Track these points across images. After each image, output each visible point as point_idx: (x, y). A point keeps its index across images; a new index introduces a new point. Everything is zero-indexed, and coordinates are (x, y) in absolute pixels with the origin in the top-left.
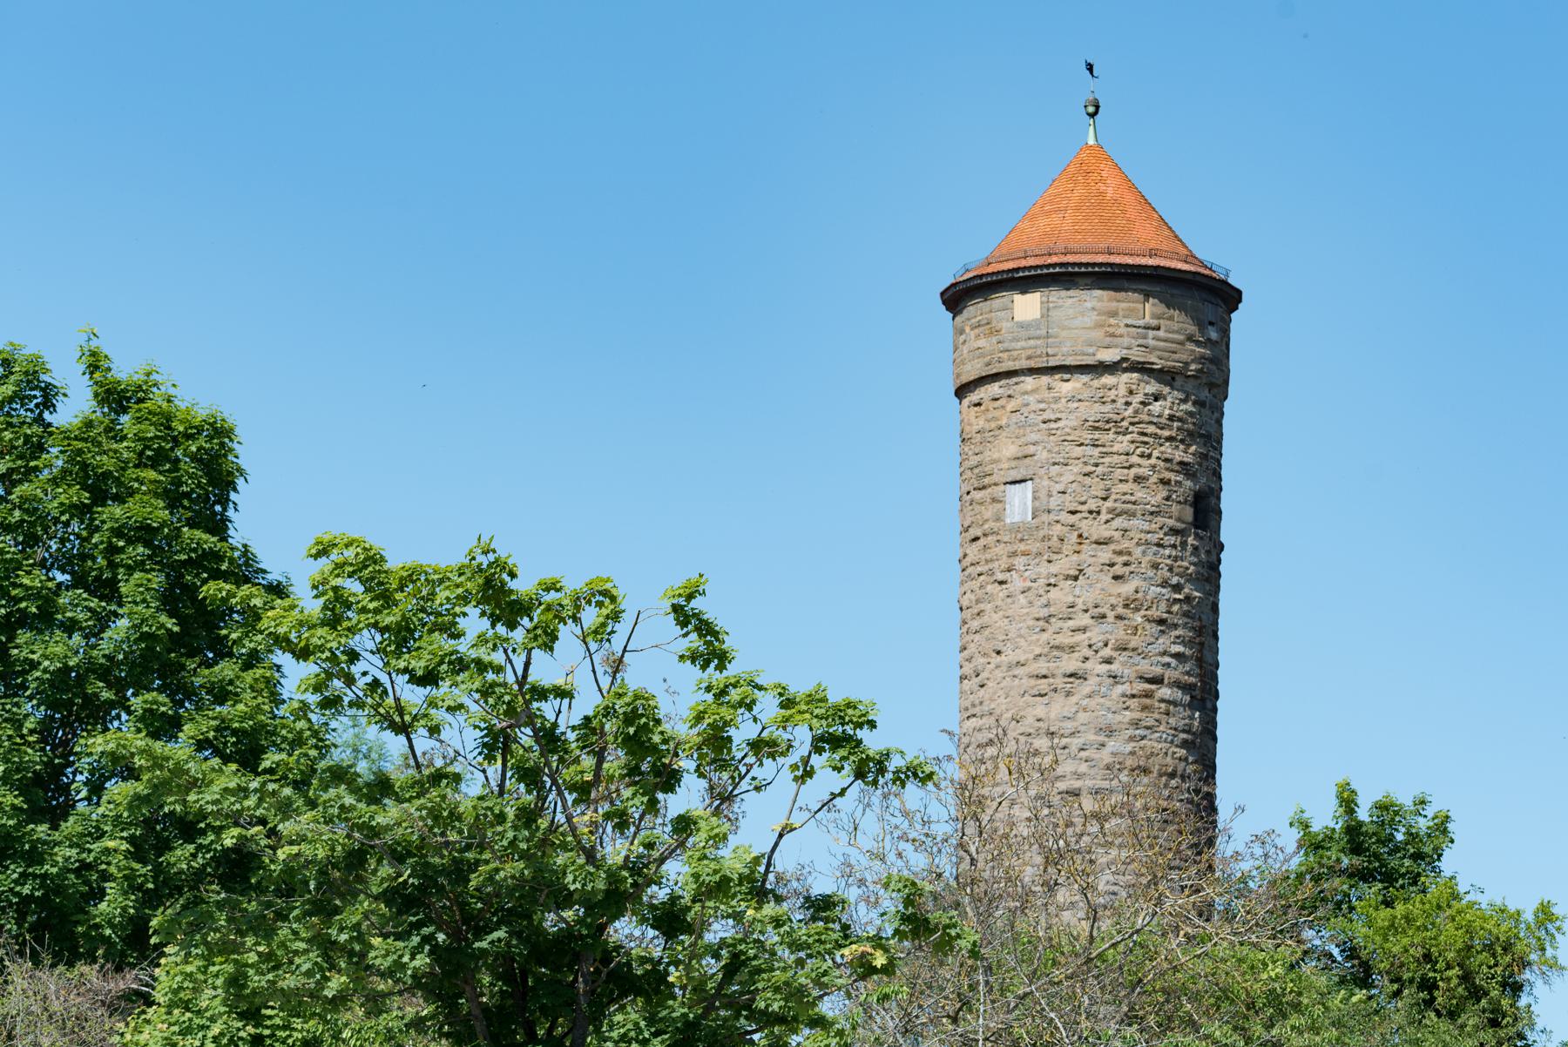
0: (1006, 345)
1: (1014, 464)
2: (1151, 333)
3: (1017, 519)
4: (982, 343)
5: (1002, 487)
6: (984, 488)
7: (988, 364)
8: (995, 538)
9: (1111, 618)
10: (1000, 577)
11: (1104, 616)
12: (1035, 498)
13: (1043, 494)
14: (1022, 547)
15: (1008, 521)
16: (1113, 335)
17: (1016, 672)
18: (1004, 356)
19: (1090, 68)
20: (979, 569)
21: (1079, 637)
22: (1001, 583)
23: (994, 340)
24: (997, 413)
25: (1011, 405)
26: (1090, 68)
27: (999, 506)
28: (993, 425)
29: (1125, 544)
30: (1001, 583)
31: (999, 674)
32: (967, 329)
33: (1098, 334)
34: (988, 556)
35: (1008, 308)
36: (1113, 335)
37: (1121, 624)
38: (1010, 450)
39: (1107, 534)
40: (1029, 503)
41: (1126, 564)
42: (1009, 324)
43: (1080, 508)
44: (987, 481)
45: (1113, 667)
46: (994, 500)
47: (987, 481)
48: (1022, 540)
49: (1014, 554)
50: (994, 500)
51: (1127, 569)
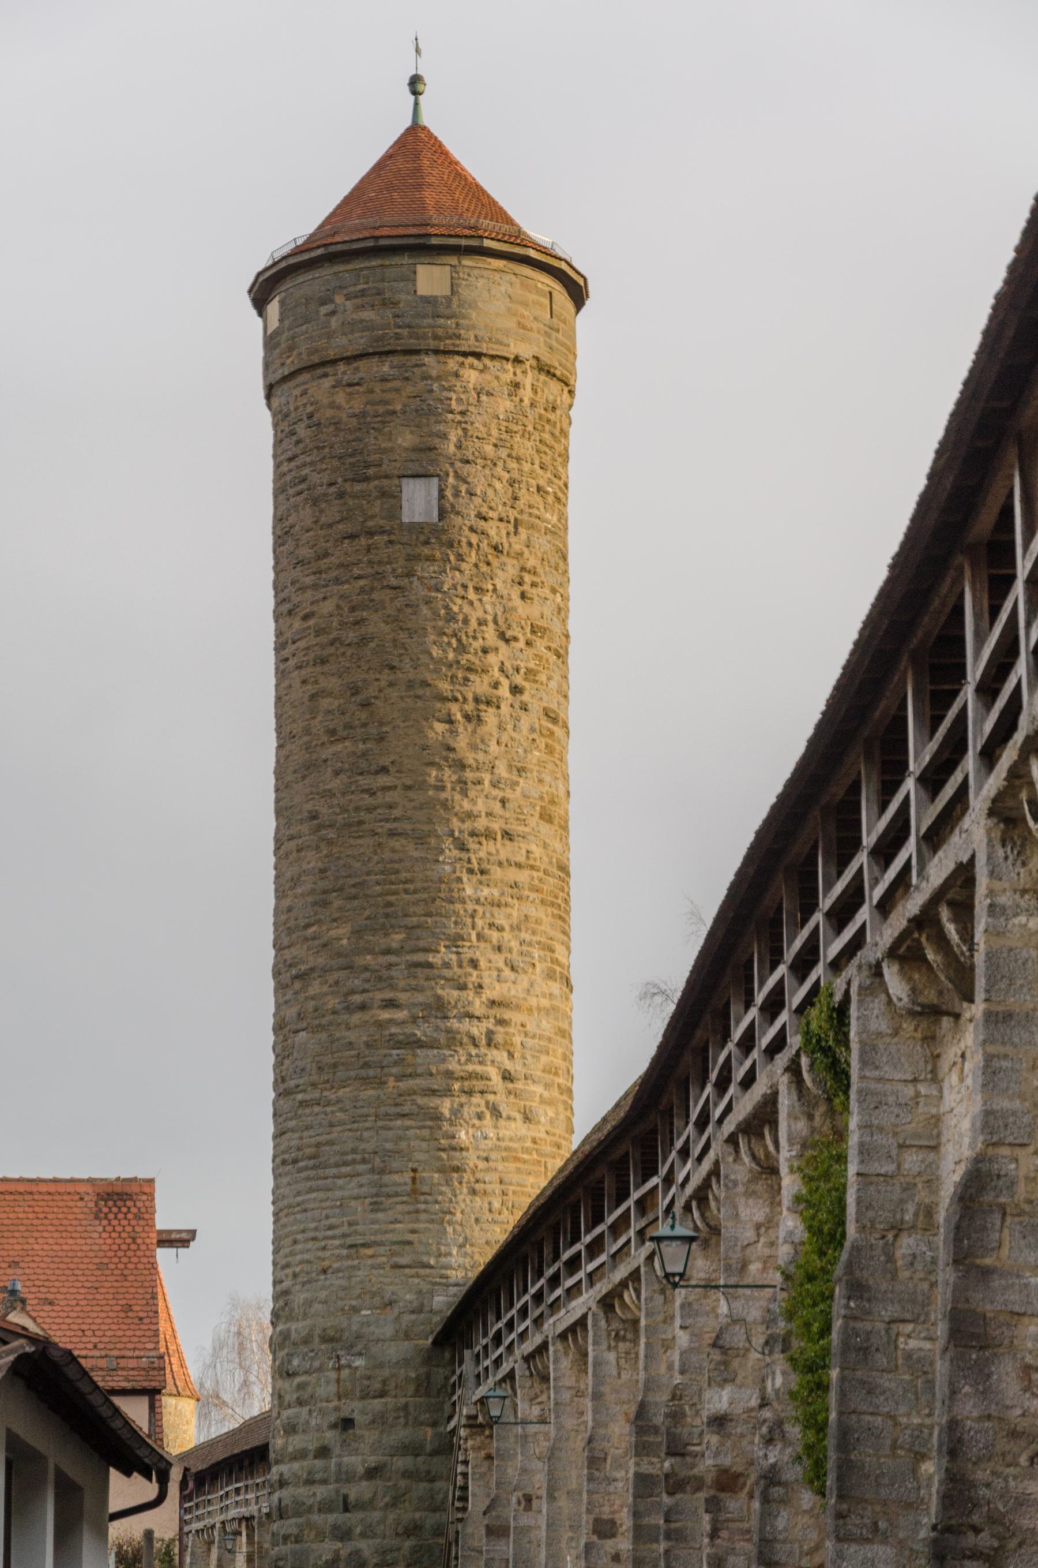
0: (407, 320)
1: (414, 456)
2: (554, 334)
3: (418, 519)
4: (368, 315)
5: (396, 481)
6: (367, 479)
7: (380, 339)
8: (386, 538)
9: (521, 644)
10: (394, 582)
11: (516, 639)
12: (442, 496)
13: (449, 493)
14: (426, 551)
15: (406, 519)
16: (524, 328)
17: (420, 692)
18: (405, 332)
19: (418, 51)
20: (356, 571)
21: (492, 659)
22: (395, 588)
23: (389, 313)
24: (388, 396)
25: (409, 389)
26: (418, 51)
27: (392, 501)
28: (381, 409)
29: (531, 563)
30: (395, 588)
31: (394, 694)
32: (339, 299)
33: (511, 324)
34: (376, 559)
35: (411, 278)
36: (524, 328)
37: (530, 652)
38: (406, 439)
39: (517, 547)
40: (435, 503)
41: (534, 585)
42: (409, 298)
43: (491, 514)
44: (371, 472)
45: (526, 697)
46: (384, 494)
47: (371, 472)
48: (427, 543)
49: (417, 558)
50: (384, 494)
51: (534, 591)
